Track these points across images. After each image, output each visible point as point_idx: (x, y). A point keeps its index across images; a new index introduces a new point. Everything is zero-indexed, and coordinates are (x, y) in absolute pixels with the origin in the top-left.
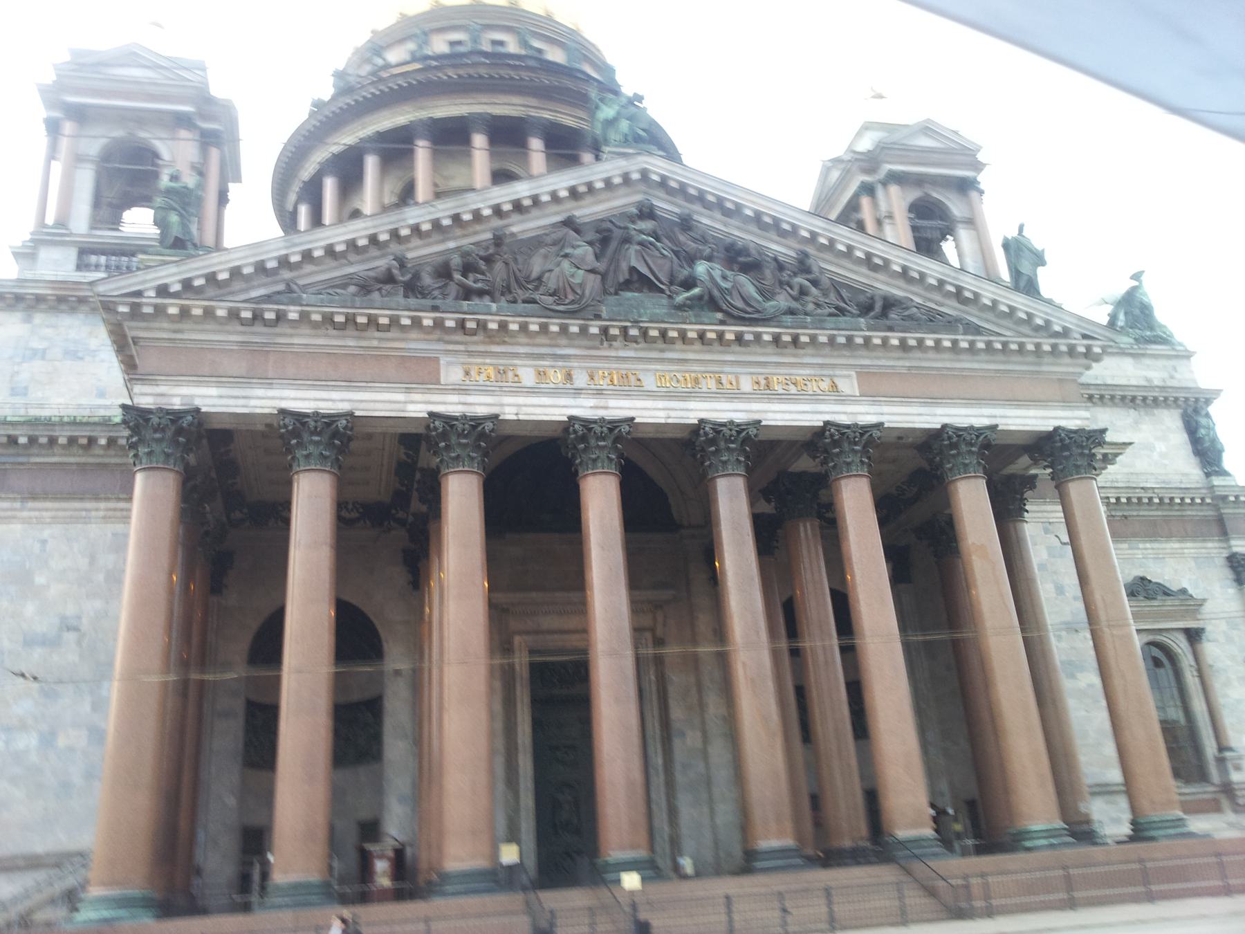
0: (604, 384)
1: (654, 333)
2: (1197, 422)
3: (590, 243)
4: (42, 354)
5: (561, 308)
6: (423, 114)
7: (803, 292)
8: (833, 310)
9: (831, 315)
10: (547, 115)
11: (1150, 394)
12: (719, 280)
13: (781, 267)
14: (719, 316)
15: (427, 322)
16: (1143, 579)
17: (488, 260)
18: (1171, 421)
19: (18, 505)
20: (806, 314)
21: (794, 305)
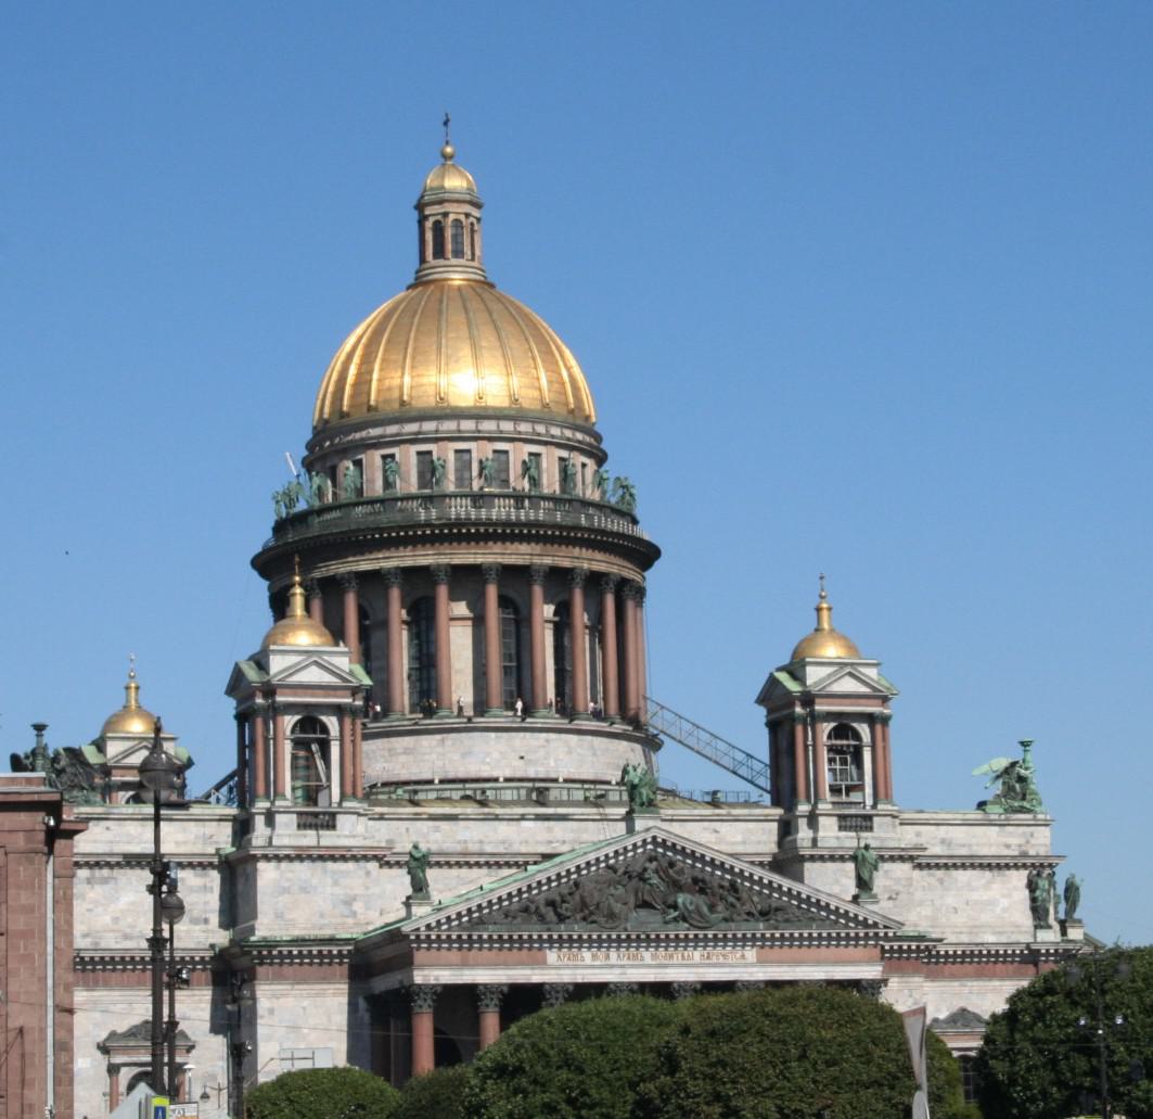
0: (625, 962)
1: (653, 937)
2: (1037, 884)
3: (624, 886)
4: (286, 891)
5: (607, 926)
6: (444, 560)
7: (733, 905)
8: (746, 917)
9: (747, 920)
10: (548, 561)
11: (1003, 862)
12: (688, 905)
13: (722, 887)
14: (687, 925)
15: (545, 937)
16: (964, 1010)
17: (570, 894)
18: (1019, 878)
19: (289, 987)
20: (733, 920)
21: (727, 914)
